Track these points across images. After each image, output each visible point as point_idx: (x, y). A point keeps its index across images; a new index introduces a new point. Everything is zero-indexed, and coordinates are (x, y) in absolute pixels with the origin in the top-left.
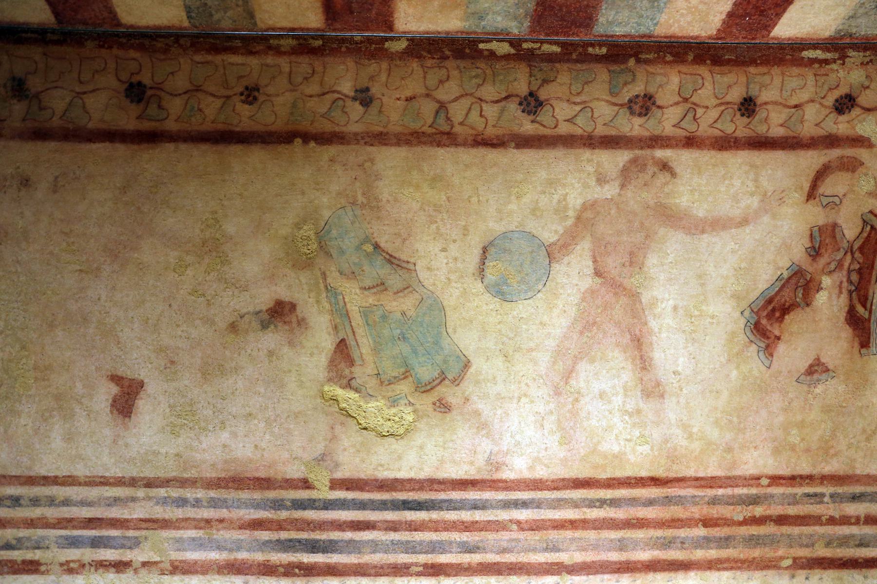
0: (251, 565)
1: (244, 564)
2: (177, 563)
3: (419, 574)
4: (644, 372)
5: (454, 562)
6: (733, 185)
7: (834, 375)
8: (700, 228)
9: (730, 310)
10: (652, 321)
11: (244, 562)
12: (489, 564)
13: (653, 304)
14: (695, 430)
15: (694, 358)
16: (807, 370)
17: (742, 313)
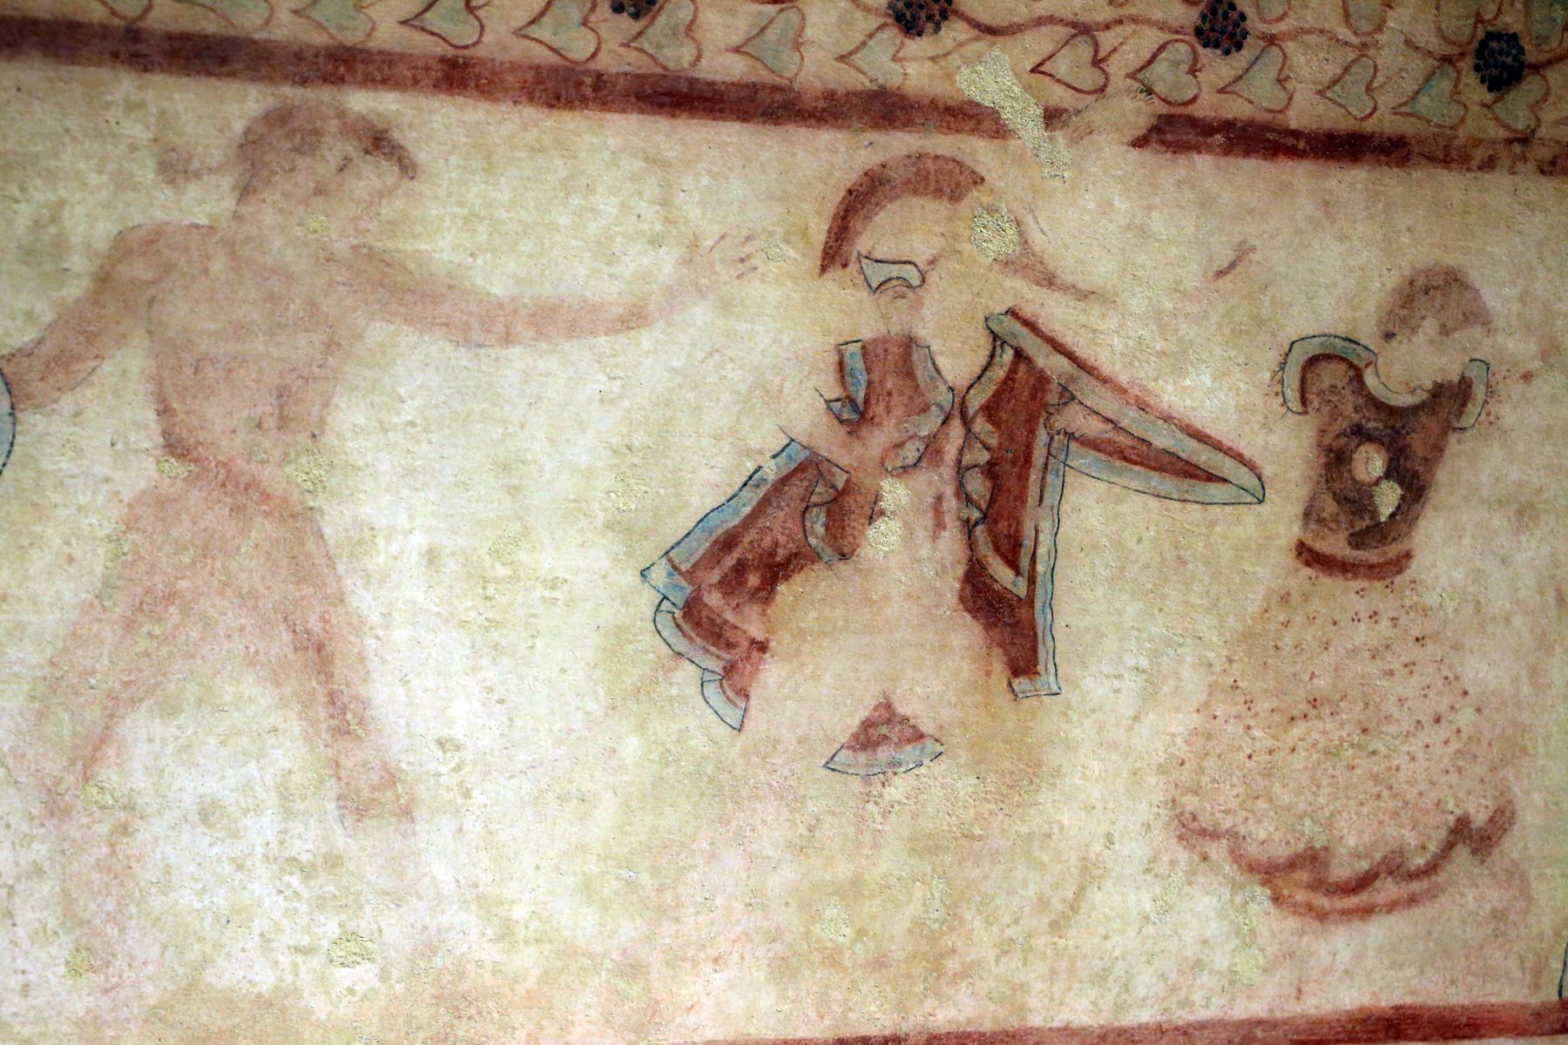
4: (345, 743)
6: (593, 210)
7: (939, 748)
8: (499, 328)
9: (606, 564)
10: (360, 591)
13: (360, 542)
14: (520, 913)
15: (501, 702)
16: (855, 737)
17: (642, 574)
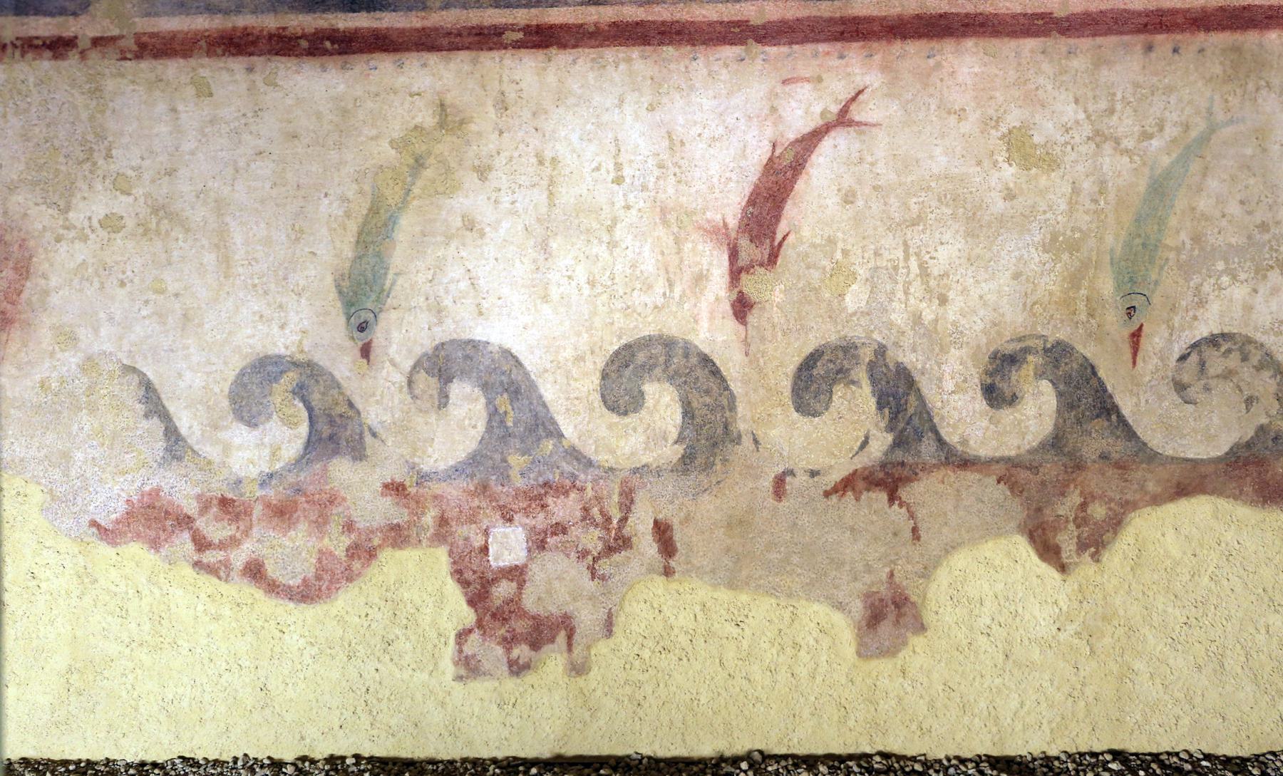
0: (258, 38)
1: (248, 35)
2: (145, 39)
3: (518, 45)
5: (571, 21)
11: (246, 32)
12: (628, 24)
